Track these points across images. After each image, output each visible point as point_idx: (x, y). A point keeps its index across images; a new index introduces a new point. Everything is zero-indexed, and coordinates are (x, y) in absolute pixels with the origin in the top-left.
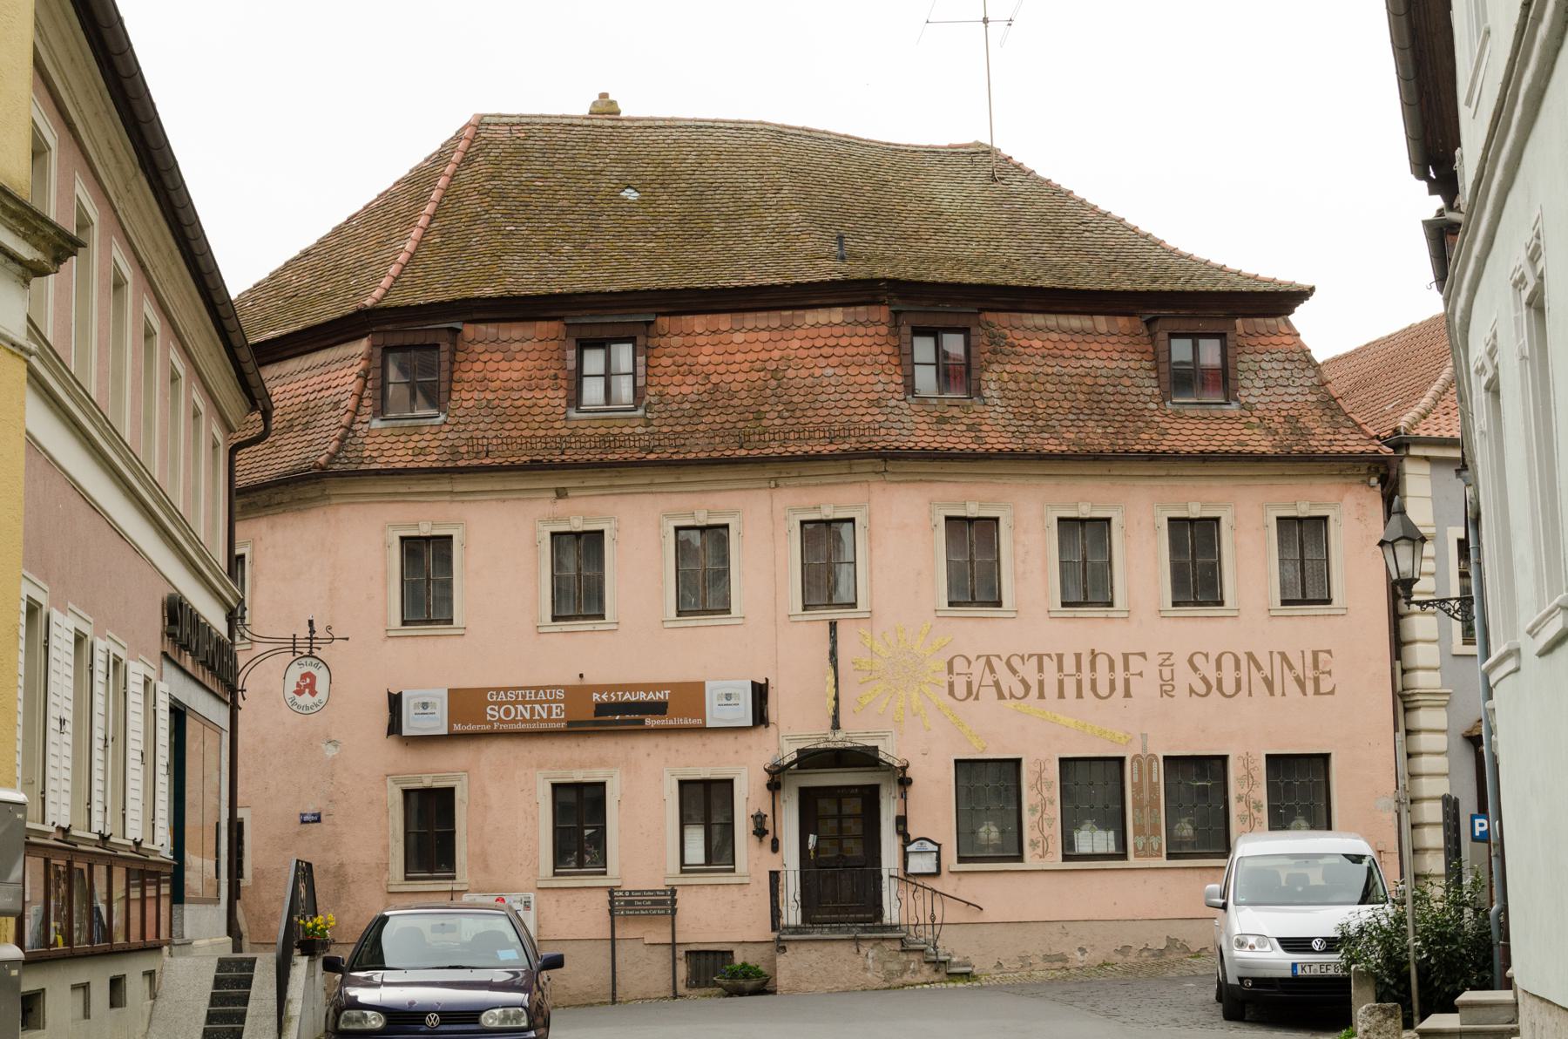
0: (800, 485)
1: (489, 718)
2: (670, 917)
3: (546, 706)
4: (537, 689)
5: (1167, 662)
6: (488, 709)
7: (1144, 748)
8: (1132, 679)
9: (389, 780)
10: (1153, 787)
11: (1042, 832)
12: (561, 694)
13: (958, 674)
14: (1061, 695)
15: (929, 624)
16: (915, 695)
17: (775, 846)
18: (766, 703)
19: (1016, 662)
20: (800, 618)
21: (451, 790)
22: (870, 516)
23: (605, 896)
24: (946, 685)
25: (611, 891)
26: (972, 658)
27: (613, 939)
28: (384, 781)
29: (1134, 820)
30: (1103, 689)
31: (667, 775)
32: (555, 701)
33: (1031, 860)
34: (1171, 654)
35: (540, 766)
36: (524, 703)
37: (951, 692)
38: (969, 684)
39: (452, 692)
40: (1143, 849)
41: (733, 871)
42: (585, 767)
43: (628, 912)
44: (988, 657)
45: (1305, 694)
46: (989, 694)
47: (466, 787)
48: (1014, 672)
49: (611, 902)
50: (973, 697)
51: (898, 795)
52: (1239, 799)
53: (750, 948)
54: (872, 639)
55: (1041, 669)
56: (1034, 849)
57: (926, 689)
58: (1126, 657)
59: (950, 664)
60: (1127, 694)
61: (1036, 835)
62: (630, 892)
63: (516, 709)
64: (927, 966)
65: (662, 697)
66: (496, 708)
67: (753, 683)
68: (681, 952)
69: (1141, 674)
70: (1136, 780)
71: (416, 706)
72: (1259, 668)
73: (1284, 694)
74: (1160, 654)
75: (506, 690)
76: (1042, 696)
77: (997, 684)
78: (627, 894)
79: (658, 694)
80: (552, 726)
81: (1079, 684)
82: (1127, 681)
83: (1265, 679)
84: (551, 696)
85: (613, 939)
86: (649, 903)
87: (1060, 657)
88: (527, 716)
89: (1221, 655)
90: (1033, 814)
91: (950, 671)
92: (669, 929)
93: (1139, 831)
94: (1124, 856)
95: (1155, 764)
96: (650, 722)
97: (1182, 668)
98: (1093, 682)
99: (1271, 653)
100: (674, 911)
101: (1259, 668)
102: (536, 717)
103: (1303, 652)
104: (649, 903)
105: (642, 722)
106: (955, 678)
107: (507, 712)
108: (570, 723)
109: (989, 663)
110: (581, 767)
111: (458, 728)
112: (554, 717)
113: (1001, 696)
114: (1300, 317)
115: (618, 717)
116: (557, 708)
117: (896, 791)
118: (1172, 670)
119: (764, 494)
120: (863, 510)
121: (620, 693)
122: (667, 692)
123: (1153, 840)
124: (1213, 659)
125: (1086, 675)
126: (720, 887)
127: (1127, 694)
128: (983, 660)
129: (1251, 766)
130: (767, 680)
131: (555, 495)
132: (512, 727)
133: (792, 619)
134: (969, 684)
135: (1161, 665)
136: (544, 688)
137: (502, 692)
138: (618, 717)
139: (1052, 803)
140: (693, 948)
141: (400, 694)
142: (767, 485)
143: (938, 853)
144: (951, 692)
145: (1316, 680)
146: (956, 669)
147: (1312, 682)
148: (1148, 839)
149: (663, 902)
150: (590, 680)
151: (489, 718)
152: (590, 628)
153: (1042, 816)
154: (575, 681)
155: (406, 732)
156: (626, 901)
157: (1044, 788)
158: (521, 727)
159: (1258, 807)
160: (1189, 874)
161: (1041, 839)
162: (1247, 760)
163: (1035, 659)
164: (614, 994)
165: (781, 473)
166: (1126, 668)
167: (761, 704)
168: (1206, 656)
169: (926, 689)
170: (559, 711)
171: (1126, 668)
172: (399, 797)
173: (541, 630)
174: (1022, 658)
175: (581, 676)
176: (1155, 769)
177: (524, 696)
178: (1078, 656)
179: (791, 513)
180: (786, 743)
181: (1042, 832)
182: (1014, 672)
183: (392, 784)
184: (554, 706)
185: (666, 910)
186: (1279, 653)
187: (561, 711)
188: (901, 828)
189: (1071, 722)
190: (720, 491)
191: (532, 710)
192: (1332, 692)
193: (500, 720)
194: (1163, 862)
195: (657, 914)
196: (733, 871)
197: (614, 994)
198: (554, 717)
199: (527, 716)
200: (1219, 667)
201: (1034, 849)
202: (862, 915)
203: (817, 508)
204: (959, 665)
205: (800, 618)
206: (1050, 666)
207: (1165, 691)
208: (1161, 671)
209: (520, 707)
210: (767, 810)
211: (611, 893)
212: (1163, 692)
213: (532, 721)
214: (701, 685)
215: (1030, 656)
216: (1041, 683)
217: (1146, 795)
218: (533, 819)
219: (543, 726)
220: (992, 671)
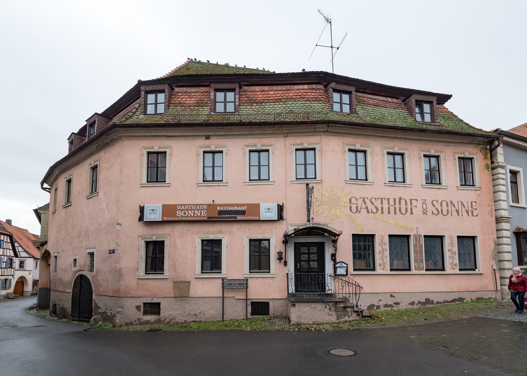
1: (177, 215)
2: (245, 290)
3: (199, 211)
4: (196, 205)
5: (425, 203)
6: (177, 212)
7: (417, 232)
8: (414, 208)
9: (140, 238)
10: (421, 246)
11: (383, 260)
12: (205, 207)
13: (353, 204)
14: (389, 213)
15: (343, 186)
16: (338, 210)
17: (285, 264)
19: (373, 200)
20: (295, 182)
21: (163, 242)
23: (220, 281)
24: (349, 207)
25: (223, 279)
26: (358, 198)
27: (223, 297)
28: (138, 238)
29: (414, 257)
30: (403, 211)
31: (245, 237)
32: (203, 209)
33: (379, 270)
34: (426, 200)
35: (197, 233)
36: (191, 210)
37: (351, 210)
38: (357, 207)
39: (163, 205)
40: (418, 267)
41: (269, 272)
42: (214, 234)
43: (229, 287)
44: (364, 198)
45: (469, 216)
46: (364, 211)
47: (169, 242)
48: (373, 204)
49: (223, 284)
50: (358, 212)
51: (332, 246)
52: (449, 251)
53: (275, 301)
54: (322, 190)
55: (382, 203)
56: (380, 267)
57: (342, 208)
58: (411, 200)
59: (350, 200)
60: (412, 213)
61: (381, 262)
62: (230, 280)
63: (188, 212)
65: (244, 209)
66: (181, 212)
67: (278, 205)
68: (249, 302)
69: (416, 206)
70: (415, 243)
71: (150, 210)
72: (454, 206)
73: (462, 216)
74: (422, 200)
75: (184, 205)
76: (382, 213)
77: (367, 208)
78: (229, 280)
79: (242, 208)
80: (202, 219)
81: (395, 209)
82: (411, 209)
83: (456, 210)
84: (202, 207)
85: (223, 297)
86: (237, 284)
87: (388, 199)
88: (192, 215)
89: (442, 201)
90: (380, 254)
91: (350, 202)
92: (245, 294)
93: (416, 261)
95: (421, 237)
96: (239, 218)
97: (430, 205)
98: (400, 208)
99: (458, 201)
100: (247, 287)
101: (454, 206)
102: (196, 215)
103: (468, 202)
104: (237, 284)
105: (236, 217)
106: (352, 205)
107: (185, 213)
108: (208, 218)
109: (364, 200)
110: (213, 234)
111: (165, 219)
112: (203, 215)
113: (368, 212)
114: (447, 105)
115: (227, 216)
116: (204, 212)
117: (331, 244)
118: (426, 206)
120: (319, 145)
121: (228, 207)
122: (246, 207)
123: (421, 264)
124: (439, 202)
125: (397, 206)
126: (264, 278)
127: (412, 213)
128: (362, 199)
129: (452, 240)
130: (283, 203)
131: (205, 138)
132: (186, 219)
134: (357, 207)
135: (423, 204)
136: (199, 205)
137: (183, 206)
138: (227, 216)
139: (386, 250)
140: (254, 301)
141: (144, 206)
142: (283, 136)
143: (347, 267)
144: (351, 210)
145: (472, 211)
146: (352, 202)
147: (471, 212)
148: (419, 264)
149: (243, 284)
150: (216, 202)
151: (177, 215)
152: (217, 184)
153: (383, 255)
154: (211, 203)
155: (145, 220)
156: (228, 283)
157: (383, 245)
158: (190, 219)
159: (455, 253)
160: (434, 277)
161: (382, 263)
162: (451, 237)
163: (380, 200)
164: (223, 318)
166: (411, 204)
167: (281, 212)
168: (437, 201)
169: (342, 208)
170: (204, 213)
171: (411, 204)
172: (143, 244)
173: (199, 185)
174: (375, 199)
175: (213, 201)
176: (421, 239)
177: (191, 208)
178: (395, 199)
181: (383, 260)
182: (373, 204)
183: (141, 239)
184: (203, 211)
185: (244, 287)
186: (460, 202)
187: (205, 213)
188: (333, 258)
189: (392, 222)
190: (266, 138)
191: (194, 213)
192: (477, 216)
193: (182, 216)
194: (424, 272)
195: (240, 288)
196: (269, 272)
197: (223, 318)
198: (203, 215)
199: (192, 215)
200: (441, 206)
201: (380, 267)
204: (354, 200)
205: (295, 182)
206: (385, 202)
207: (424, 213)
208: (423, 206)
209: (190, 211)
210: (283, 250)
211: (223, 280)
212: (424, 213)
213: (194, 216)
214: (258, 205)
215: (378, 198)
216: (382, 208)
217: (418, 249)
218: (194, 252)
219: (198, 219)
220: (365, 203)
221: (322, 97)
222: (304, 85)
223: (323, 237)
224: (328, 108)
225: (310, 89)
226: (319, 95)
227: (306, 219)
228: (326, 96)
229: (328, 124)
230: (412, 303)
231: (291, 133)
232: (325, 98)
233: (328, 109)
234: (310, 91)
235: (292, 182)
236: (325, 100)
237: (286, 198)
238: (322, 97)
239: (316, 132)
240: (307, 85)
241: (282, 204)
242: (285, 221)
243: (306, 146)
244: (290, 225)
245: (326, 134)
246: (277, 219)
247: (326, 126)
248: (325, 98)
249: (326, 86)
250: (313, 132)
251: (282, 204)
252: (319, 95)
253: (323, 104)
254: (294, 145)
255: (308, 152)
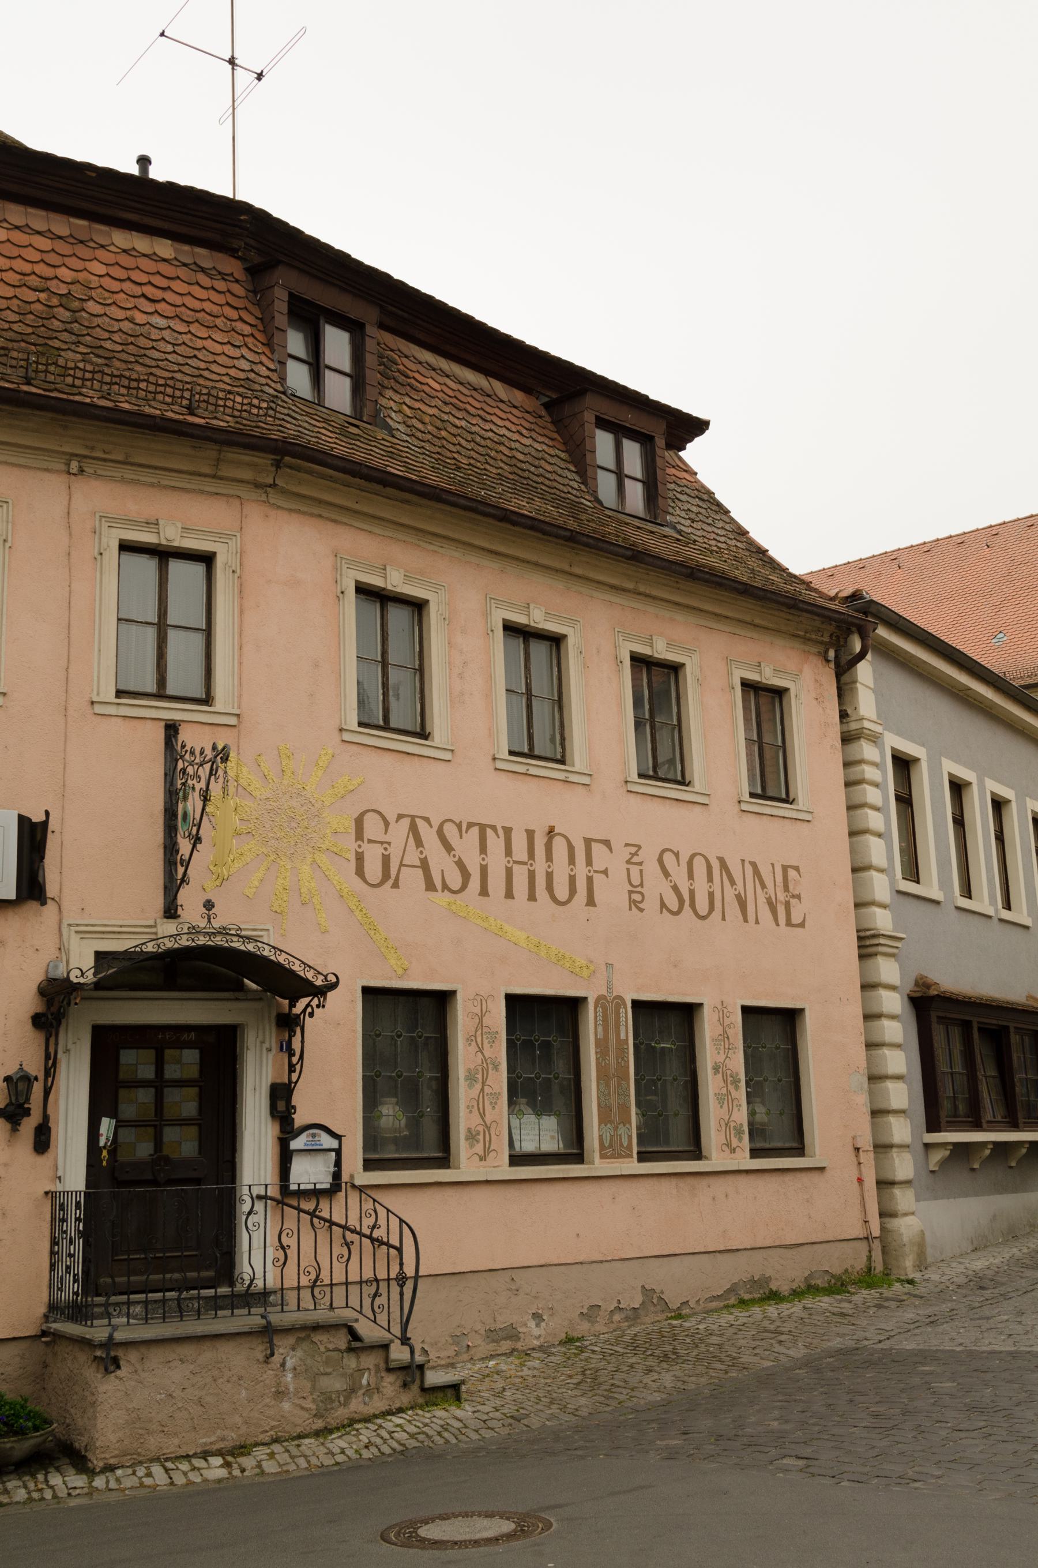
0: (123, 480)
5: (635, 859)
7: (610, 988)
8: (598, 879)
10: (622, 1044)
11: (482, 1116)
13: (370, 841)
14: (509, 894)
15: (330, 751)
16: (306, 869)
18: (43, 858)
19: (450, 831)
22: (242, 554)
24: (352, 857)
26: (391, 818)
29: (598, 1098)
30: (562, 891)
34: (639, 847)
37: (360, 872)
38: (386, 860)
40: (611, 1146)
44: (413, 818)
45: (778, 925)
46: (412, 878)
48: (448, 848)
50: (391, 882)
51: (275, 1046)
52: (716, 1069)
55: (483, 849)
56: (472, 1146)
57: (323, 859)
58: (588, 842)
59: (359, 822)
60: (591, 902)
61: (475, 1120)
64: (390, 1378)
67: (23, 820)
69: (605, 872)
70: (600, 1036)
72: (733, 883)
73: (757, 922)
74: (627, 845)
76: (484, 892)
77: (425, 865)
81: (532, 875)
82: (590, 880)
83: (738, 897)
87: (508, 831)
89: (693, 857)
90: (471, 1086)
91: (359, 835)
93: (605, 1118)
94: (579, 1158)
95: (622, 1010)
97: (652, 868)
98: (549, 876)
99: (743, 861)
101: (733, 883)
103: (773, 865)
106: (366, 847)
109: (414, 829)
113: (430, 886)
117: (272, 1036)
118: (641, 871)
119: (55, 483)
120: (232, 543)
123: (622, 1130)
124: (684, 858)
125: (540, 866)
127: (591, 902)
128: (406, 823)
129: (727, 1021)
130: (47, 813)
133: (98, 709)
134: (386, 860)
135: (628, 862)
139: (496, 1067)
142: (63, 467)
143: (338, 1152)
144: (360, 872)
145: (787, 905)
146: (369, 833)
147: (783, 907)
148: (616, 1129)
153: (482, 1090)
157: (486, 1042)
159: (736, 1082)
160: (666, 1184)
161: (481, 1129)
162: (722, 1009)
163: (475, 830)
165: (93, 448)
166: (589, 862)
168: (677, 855)
169: (323, 859)
171: (589, 862)
174: (459, 826)
176: (622, 1015)
178: (530, 834)
179: (105, 525)
180: (75, 939)
181: (482, 1116)
182: (448, 848)
186: (750, 862)
188: (281, 1106)
189: (520, 936)
192: (802, 925)
194: (633, 1166)
200: (691, 876)
201: (472, 1146)
202: (195, 1274)
203: (153, 524)
204: (372, 827)
206: (496, 844)
207: (635, 902)
208: (628, 870)
212: (633, 903)
215: (470, 825)
216: (484, 870)
217: (612, 1059)
220: (419, 843)
221: (241, 319)
222: (155, 238)
223: (237, 999)
224: (268, 377)
225: (185, 265)
226: (228, 304)
227: (158, 901)
228: (257, 318)
229: (278, 458)
230: (591, 1313)
231: (105, 460)
232: (251, 325)
233: (270, 382)
234: (182, 272)
235: (98, 709)
236: (252, 335)
237: (64, 786)
238: (241, 319)
239: (221, 478)
240: (170, 242)
241: (38, 817)
242: (50, 907)
243: (172, 535)
244: (76, 932)
245: (264, 498)
246: (12, 895)
247: (270, 462)
248: (251, 325)
249: (254, 272)
250: (205, 476)
251: (44, 818)
252: (228, 304)
253: (244, 351)
254: (114, 521)
255: (176, 567)
